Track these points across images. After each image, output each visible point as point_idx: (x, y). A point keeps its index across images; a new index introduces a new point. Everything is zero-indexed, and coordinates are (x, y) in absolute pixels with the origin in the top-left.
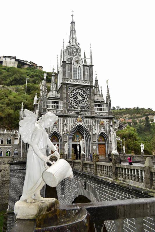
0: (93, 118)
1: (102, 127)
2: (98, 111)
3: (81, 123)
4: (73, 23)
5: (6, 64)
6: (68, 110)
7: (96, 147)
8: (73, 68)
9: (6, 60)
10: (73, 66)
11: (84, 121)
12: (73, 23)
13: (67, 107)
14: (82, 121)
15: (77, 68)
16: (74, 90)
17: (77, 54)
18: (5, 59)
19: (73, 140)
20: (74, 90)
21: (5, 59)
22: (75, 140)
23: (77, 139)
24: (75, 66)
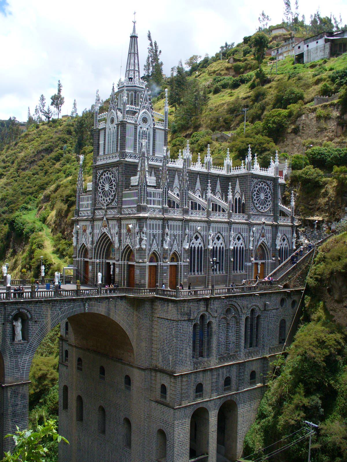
0: (119, 220)
1: (128, 237)
2: (129, 206)
3: (106, 229)
5: (309, 57)
6: (95, 209)
7: (119, 269)
9: (310, 48)
10: (107, 130)
11: (110, 225)
13: (95, 205)
14: (106, 226)
16: (102, 174)
18: (308, 46)
19: (108, 257)
20: (102, 174)
21: (308, 46)
22: (111, 256)
23: (112, 255)
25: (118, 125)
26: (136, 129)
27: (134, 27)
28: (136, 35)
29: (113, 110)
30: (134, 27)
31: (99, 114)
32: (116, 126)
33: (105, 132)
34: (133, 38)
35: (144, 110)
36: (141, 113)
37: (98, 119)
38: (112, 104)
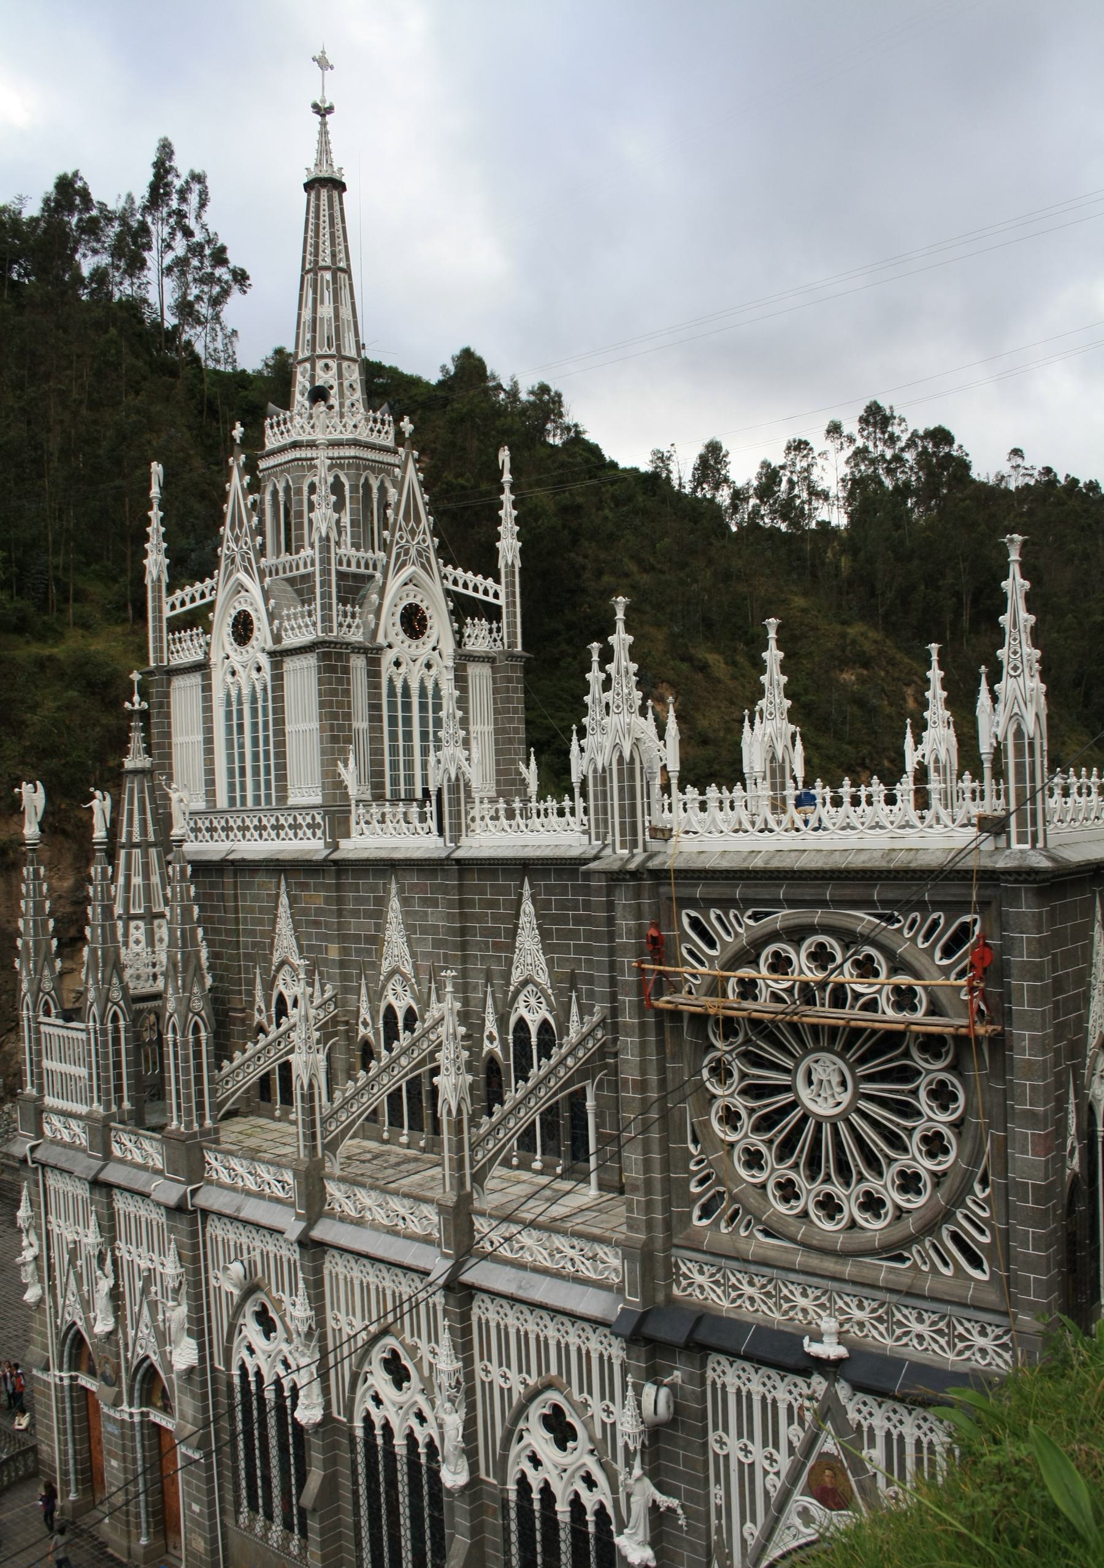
4: (326, 186)
8: (218, 695)
10: (219, 677)
12: (326, 186)
15: (246, 691)
17: (238, 559)
24: (233, 673)
25: (278, 657)
26: (374, 674)
27: (324, 132)
28: (337, 176)
29: (242, 576)
30: (324, 132)
31: (171, 591)
32: (265, 661)
33: (207, 688)
34: (324, 193)
35: (408, 571)
36: (394, 584)
37: (167, 613)
38: (237, 540)
